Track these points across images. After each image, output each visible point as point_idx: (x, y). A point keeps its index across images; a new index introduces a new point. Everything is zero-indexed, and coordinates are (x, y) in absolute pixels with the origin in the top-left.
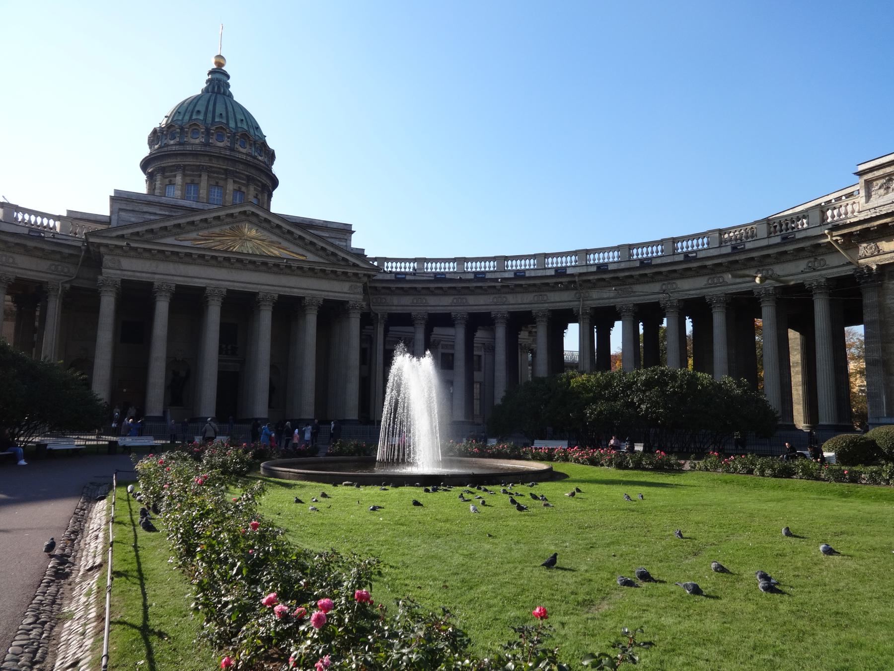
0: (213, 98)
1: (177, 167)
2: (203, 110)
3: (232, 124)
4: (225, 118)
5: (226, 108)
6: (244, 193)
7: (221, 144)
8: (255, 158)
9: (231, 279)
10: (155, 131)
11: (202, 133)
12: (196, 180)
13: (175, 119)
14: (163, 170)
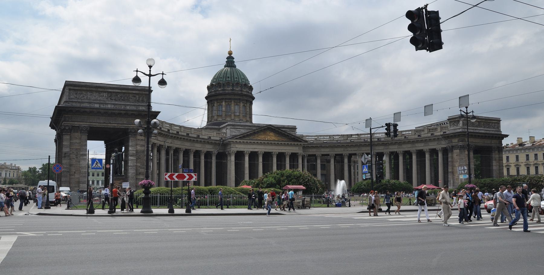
0: (232, 70)
1: (222, 99)
2: (230, 76)
3: (240, 81)
4: (238, 79)
5: (237, 74)
6: (245, 106)
7: (237, 89)
8: (248, 92)
9: (265, 148)
10: (212, 85)
11: (231, 86)
12: (230, 103)
13: (220, 80)
14: (217, 100)
